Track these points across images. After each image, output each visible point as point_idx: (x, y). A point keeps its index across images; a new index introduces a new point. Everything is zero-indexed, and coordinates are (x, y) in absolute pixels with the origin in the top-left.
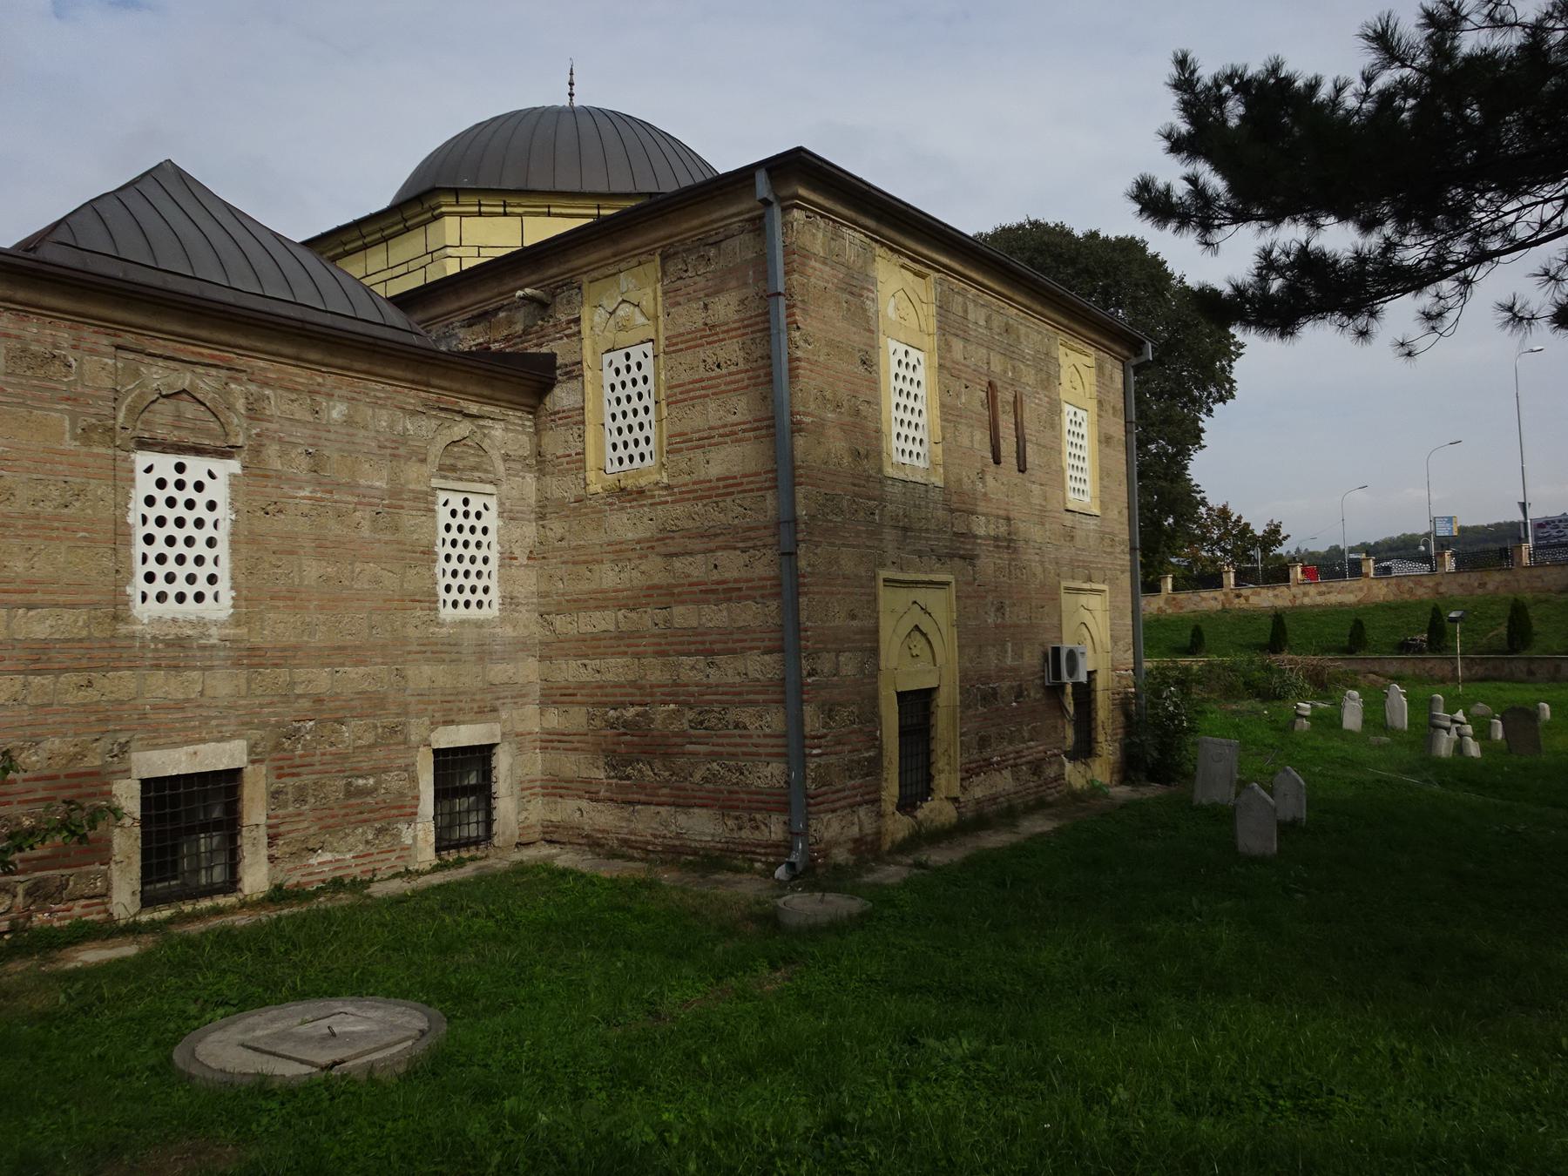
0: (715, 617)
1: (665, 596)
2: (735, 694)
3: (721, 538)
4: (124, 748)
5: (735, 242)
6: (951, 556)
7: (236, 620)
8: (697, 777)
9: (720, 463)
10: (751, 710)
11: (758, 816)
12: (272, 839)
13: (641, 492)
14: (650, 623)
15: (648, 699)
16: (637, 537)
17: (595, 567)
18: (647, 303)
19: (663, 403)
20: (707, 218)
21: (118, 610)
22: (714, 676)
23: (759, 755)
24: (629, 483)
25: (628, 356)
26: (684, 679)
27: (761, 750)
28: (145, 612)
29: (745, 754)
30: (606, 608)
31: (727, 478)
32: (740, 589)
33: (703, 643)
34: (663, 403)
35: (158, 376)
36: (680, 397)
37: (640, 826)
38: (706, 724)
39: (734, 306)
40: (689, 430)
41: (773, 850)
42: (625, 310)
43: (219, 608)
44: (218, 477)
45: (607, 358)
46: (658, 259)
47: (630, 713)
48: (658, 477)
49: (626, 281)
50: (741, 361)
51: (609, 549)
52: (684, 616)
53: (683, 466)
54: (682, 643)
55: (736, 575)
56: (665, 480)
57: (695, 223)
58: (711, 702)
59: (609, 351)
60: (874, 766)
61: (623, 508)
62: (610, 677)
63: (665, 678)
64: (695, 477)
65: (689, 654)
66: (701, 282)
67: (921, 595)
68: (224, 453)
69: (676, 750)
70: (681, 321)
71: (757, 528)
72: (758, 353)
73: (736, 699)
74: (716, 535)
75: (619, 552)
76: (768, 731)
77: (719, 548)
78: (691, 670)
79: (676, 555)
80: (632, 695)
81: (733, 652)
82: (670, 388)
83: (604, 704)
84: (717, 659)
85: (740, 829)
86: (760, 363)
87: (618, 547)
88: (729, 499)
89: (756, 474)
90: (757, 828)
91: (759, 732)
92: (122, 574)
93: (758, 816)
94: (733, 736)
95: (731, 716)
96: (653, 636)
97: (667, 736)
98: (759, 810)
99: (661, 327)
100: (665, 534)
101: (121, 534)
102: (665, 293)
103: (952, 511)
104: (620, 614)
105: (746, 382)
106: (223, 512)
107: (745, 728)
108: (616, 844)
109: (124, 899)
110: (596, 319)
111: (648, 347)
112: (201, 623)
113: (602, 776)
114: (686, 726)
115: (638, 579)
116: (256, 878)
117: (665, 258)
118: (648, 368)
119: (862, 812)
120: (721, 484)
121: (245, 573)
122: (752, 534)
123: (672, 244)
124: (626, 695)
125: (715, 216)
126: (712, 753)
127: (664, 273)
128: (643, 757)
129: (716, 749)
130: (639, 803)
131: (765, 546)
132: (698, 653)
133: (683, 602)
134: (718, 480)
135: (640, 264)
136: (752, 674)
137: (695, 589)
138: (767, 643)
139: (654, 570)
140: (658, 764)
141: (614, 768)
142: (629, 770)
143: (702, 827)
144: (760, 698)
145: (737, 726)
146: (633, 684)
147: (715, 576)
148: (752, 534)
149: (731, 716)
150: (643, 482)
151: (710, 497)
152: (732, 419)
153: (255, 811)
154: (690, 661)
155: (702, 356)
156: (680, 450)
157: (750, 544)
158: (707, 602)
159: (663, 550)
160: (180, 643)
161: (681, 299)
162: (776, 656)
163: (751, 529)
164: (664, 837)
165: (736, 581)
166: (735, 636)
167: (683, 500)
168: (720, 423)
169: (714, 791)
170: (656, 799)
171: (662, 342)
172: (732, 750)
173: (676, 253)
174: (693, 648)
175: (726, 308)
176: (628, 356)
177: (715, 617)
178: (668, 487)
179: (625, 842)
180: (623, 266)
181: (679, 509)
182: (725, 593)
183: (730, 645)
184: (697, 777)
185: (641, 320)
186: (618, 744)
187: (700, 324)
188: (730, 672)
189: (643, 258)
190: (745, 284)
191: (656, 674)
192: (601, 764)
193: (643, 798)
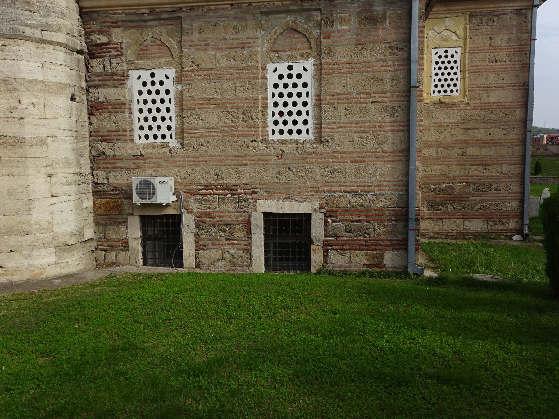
0: (488, 152)
1: (466, 144)
2: (496, 179)
3: (493, 124)
5: (508, 16)
8: (476, 208)
9: (494, 97)
10: (503, 185)
11: (504, 220)
13: (454, 104)
14: (455, 154)
15: (453, 181)
16: (449, 121)
17: (426, 131)
18: (460, 32)
19: (467, 72)
20: (497, 5)
22: (486, 173)
23: (506, 199)
24: (447, 101)
25: (446, 52)
26: (471, 173)
27: (507, 198)
29: (499, 199)
30: (432, 147)
31: (498, 103)
32: (501, 143)
33: (482, 161)
34: (467, 72)
36: (475, 71)
37: (445, 227)
38: (481, 189)
39: (505, 39)
40: (480, 83)
41: (510, 231)
42: (446, 33)
45: (434, 51)
46: (467, 16)
47: (442, 186)
48: (461, 99)
49: (449, 22)
50: (507, 61)
51: (434, 125)
52: (471, 151)
53: (476, 96)
54: (470, 161)
55: (499, 137)
56: (467, 101)
57: (492, 6)
58: (484, 182)
59: (436, 48)
61: (443, 110)
62: (433, 173)
63: (462, 173)
64: (482, 101)
65: (474, 165)
66: (489, 29)
69: (466, 199)
70: (478, 42)
71: (511, 122)
72: (517, 58)
73: (496, 181)
74: (491, 123)
75: (440, 128)
76: (511, 191)
77: (491, 128)
78: (475, 171)
79: (470, 129)
80: (444, 180)
81: (497, 164)
82: (470, 66)
83: (429, 183)
84: (488, 167)
85: (495, 225)
86: (516, 63)
87: (439, 125)
88: (498, 110)
89: (512, 102)
90: (503, 224)
91: (507, 192)
93: (504, 220)
94: (495, 194)
95: (494, 187)
96: (457, 158)
97: (462, 195)
98: (503, 218)
99: (468, 43)
100: (465, 121)
102: (470, 30)
104: (439, 150)
105: (509, 69)
107: (500, 190)
108: (432, 234)
110: (430, 34)
111: (458, 50)
113: (426, 210)
114: (471, 190)
115: (450, 138)
117: (471, 16)
118: (457, 57)
120: (495, 105)
122: (509, 124)
123: (475, 12)
124: (441, 180)
125: (502, 5)
126: (484, 200)
127: (470, 22)
128: (448, 202)
129: (486, 198)
130: (445, 219)
131: (514, 128)
132: (478, 165)
133: (472, 146)
134: (493, 103)
135: (457, 16)
136: (504, 171)
137: (479, 142)
138: (512, 161)
139: (459, 133)
140: (456, 205)
141: (432, 206)
142: (441, 207)
143: (476, 225)
144: (508, 180)
145: (496, 190)
146: (445, 176)
147: (490, 137)
148: (509, 124)
149: (494, 187)
150: (455, 101)
151: (489, 109)
152: (502, 82)
154: (476, 167)
155: (488, 57)
156: (476, 90)
157: (507, 127)
158: (485, 147)
159: (463, 127)
161: (479, 34)
162: (516, 166)
163: (507, 122)
164: (458, 230)
165: (499, 139)
166: (498, 159)
167: (476, 109)
168: (495, 82)
169: (484, 213)
170: (453, 217)
171: (468, 49)
172: (494, 198)
173: (478, 15)
174: (477, 163)
175: (501, 40)
176: (446, 52)
177: (488, 152)
178: (468, 104)
179: (437, 233)
180: (448, 15)
181: (473, 112)
182: (496, 144)
183: (495, 162)
184: (476, 208)
185: (454, 38)
186: (435, 198)
187: (488, 44)
188: (494, 172)
189: (460, 14)
190: (512, 33)
191: (457, 172)
192: (426, 205)
193: (447, 217)
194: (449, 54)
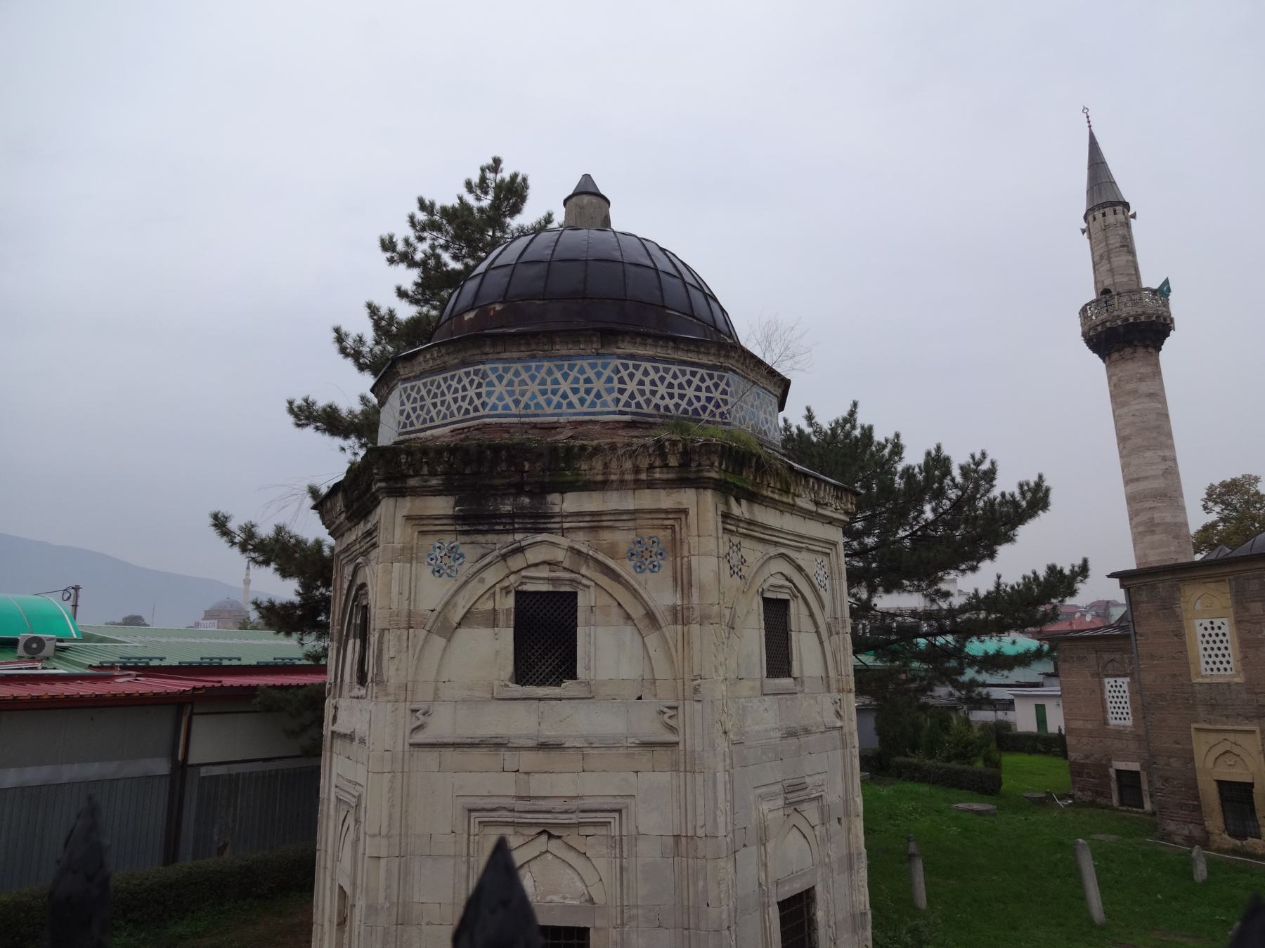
4: (1110, 760)
6: (1259, 717)
7: (1134, 726)
12: (1151, 796)
21: (1106, 723)
28: (1112, 722)
35: (1106, 657)
43: (1129, 723)
44: (1124, 682)
60: (1198, 808)
67: (1231, 737)
68: (1125, 676)
92: (1104, 710)
101: (1103, 701)
103: (1256, 694)
106: (1127, 694)
109: (1115, 801)
112: (1125, 726)
116: (1148, 806)
119: (1191, 826)
121: (1134, 711)
153: (1145, 787)
160: (1119, 732)
194: (1215, 626)
